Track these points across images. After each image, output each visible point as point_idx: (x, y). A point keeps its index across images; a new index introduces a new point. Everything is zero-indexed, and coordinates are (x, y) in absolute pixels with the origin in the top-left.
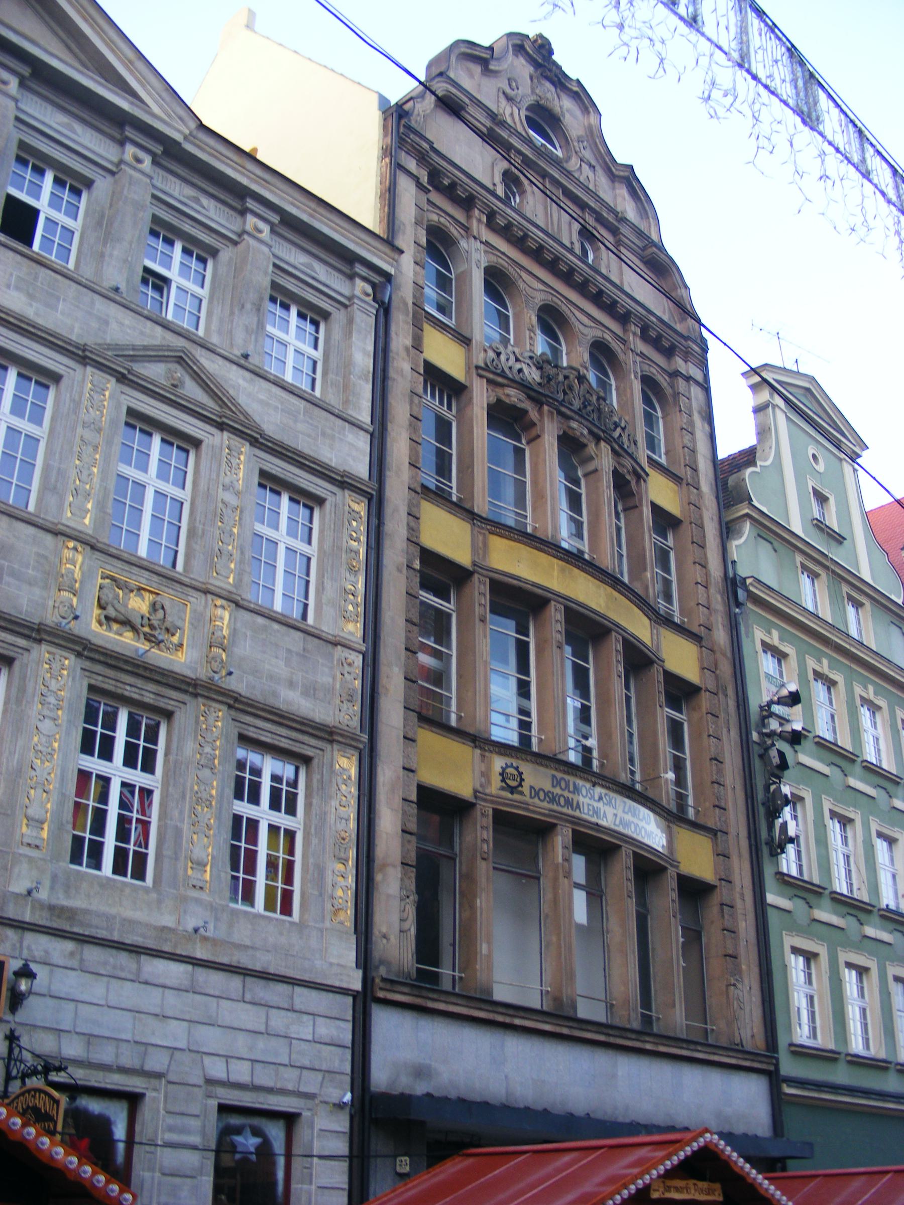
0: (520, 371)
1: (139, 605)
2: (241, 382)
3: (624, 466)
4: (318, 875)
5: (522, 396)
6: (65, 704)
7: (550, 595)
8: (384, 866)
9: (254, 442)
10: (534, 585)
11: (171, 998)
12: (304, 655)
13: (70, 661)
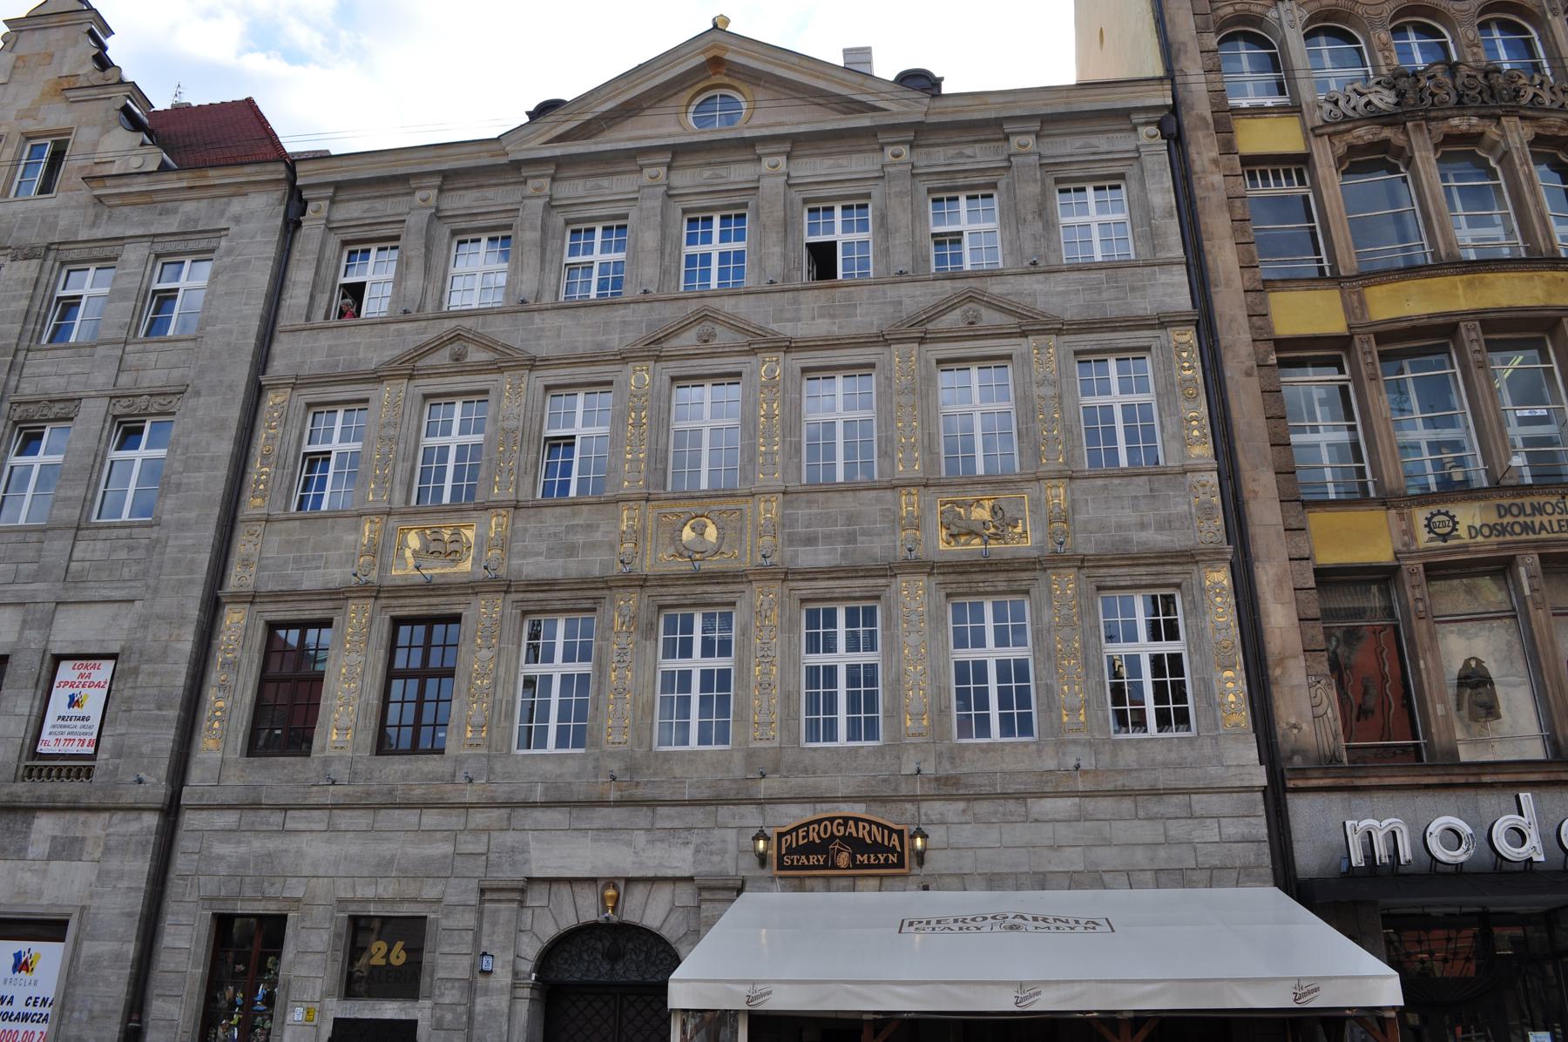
0: (1369, 103)
1: (982, 514)
2: (1036, 286)
3: (1549, 126)
4: (1206, 685)
5: (1375, 128)
6: (926, 617)
7: (1454, 319)
8: (1281, 661)
9: (1059, 332)
10: (1430, 316)
11: (1062, 829)
12: (1153, 495)
13: (922, 581)
